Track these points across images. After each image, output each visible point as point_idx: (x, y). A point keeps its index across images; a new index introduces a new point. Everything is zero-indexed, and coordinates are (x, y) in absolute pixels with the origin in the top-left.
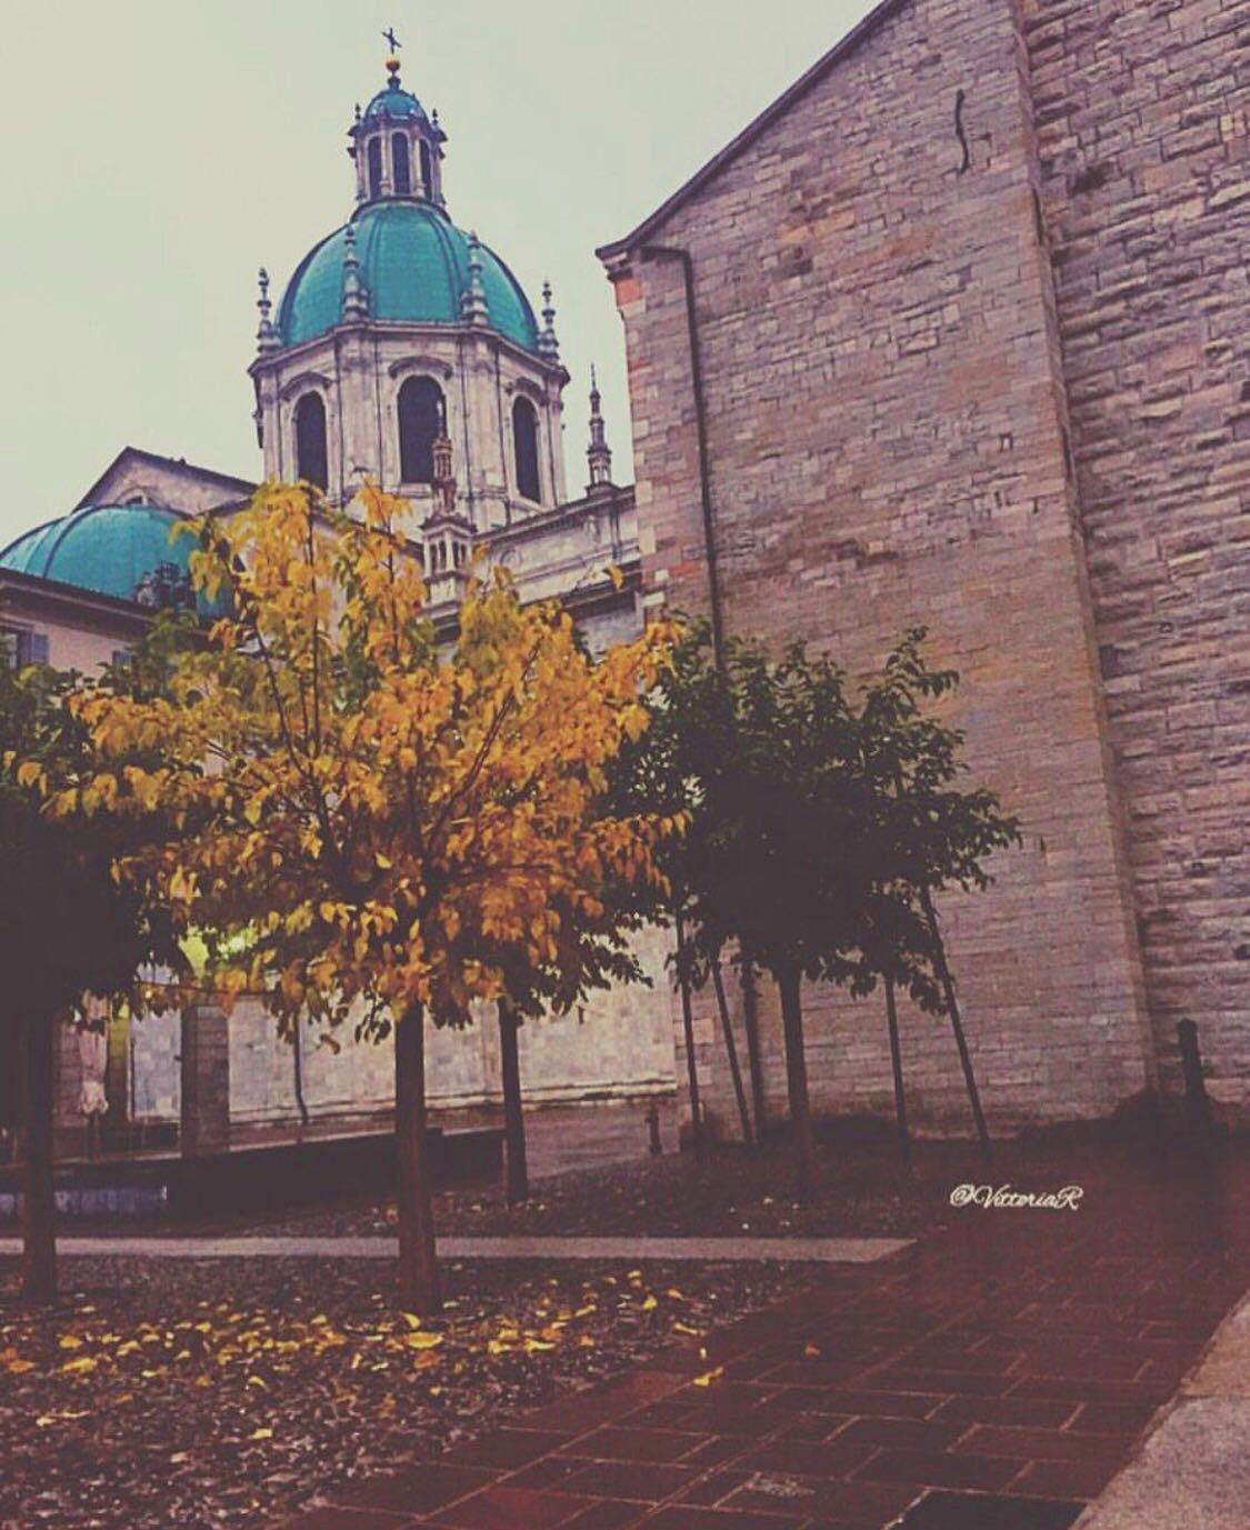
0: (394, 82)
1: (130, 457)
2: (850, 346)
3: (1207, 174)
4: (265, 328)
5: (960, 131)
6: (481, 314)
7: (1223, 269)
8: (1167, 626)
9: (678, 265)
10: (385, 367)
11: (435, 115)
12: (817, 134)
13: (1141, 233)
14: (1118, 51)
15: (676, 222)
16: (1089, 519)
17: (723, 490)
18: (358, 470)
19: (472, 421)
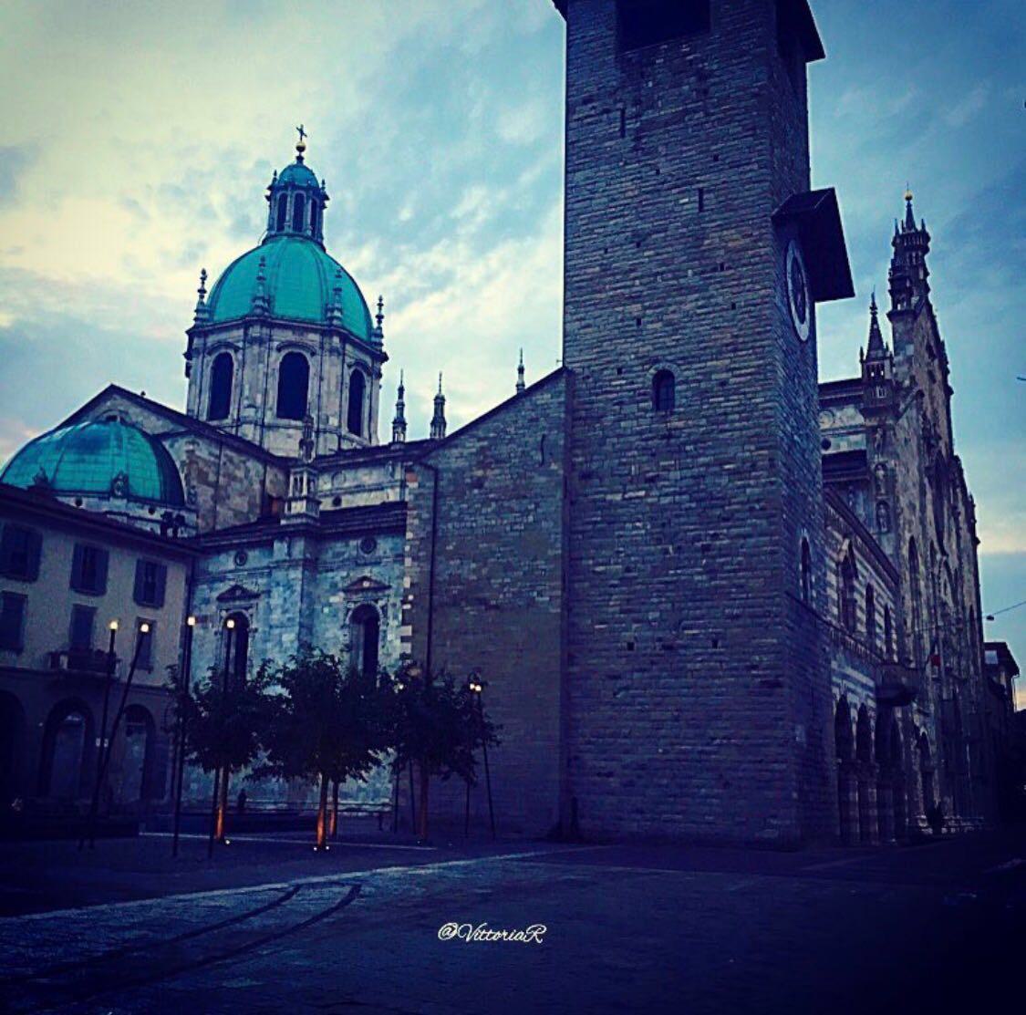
0: (300, 159)
1: (113, 391)
2: (493, 522)
4: (201, 307)
6: (338, 318)
7: (625, 522)
8: (591, 651)
9: (431, 472)
10: (275, 344)
11: (323, 183)
14: (603, 430)
18: (250, 406)
19: (324, 384)
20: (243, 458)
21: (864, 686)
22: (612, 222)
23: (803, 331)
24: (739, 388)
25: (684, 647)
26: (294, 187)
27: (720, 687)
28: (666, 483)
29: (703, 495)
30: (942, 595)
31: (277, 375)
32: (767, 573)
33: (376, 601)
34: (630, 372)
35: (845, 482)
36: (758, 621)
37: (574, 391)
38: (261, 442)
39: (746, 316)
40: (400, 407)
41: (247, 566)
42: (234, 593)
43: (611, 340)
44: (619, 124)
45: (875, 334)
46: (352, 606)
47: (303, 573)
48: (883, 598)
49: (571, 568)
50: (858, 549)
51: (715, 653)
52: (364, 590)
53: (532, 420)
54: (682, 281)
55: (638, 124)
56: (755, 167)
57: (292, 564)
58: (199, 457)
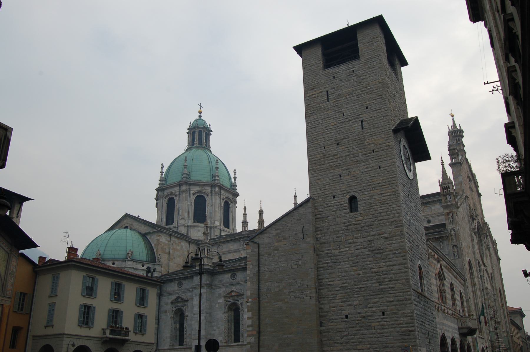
0: (200, 116)
1: (127, 216)
3: (339, 246)
4: (161, 179)
5: (303, 232)
6: (218, 180)
7: (341, 262)
9: (257, 245)
10: (192, 192)
11: (210, 125)
12: (281, 227)
13: (329, 253)
14: (328, 222)
16: (320, 299)
17: (262, 286)
18: (182, 219)
20: (180, 241)
21: (452, 328)
22: (327, 136)
23: (411, 176)
24: (385, 202)
25: (369, 316)
26: (198, 127)
27: (387, 333)
28: (357, 244)
29: (374, 248)
30: (486, 285)
31: (193, 205)
32: (404, 281)
33: (238, 301)
34: (338, 197)
35: (438, 238)
36: (401, 302)
37: (315, 207)
38: (187, 234)
39: (385, 171)
40: (245, 215)
41: (183, 288)
42: (178, 300)
43: (329, 184)
44: (326, 96)
45: (444, 173)
46: (228, 303)
47: (206, 290)
48: (458, 287)
49: (319, 285)
50: (445, 267)
51: (384, 318)
52: (232, 296)
53: (298, 220)
54: (357, 158)
55: (334, 96)
56: (383, 110)
58: (162, 242)
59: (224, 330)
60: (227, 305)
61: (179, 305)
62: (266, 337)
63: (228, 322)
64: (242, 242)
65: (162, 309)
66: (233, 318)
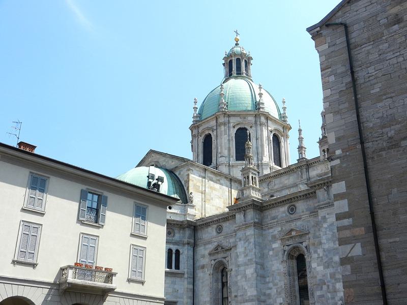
0: (237, 44)
1: (152, 152)
9: (343, 28)
10: (231, 125)
15: (340, 13)
17: (365, 114)
18: (221, 157)
26: (235, 55)
40: (301, 139)
41: (222, 234)
42: (217, 250)
46: (287, 248)
52: (291, 237)
57: (247, 226)
59: (283, 287)
60: (285, 251)
61: (220, 256)
62: (397, 239)
63: (290, 276)
64: (299, 172)
65: (198, 264)
66: (296, 270)
